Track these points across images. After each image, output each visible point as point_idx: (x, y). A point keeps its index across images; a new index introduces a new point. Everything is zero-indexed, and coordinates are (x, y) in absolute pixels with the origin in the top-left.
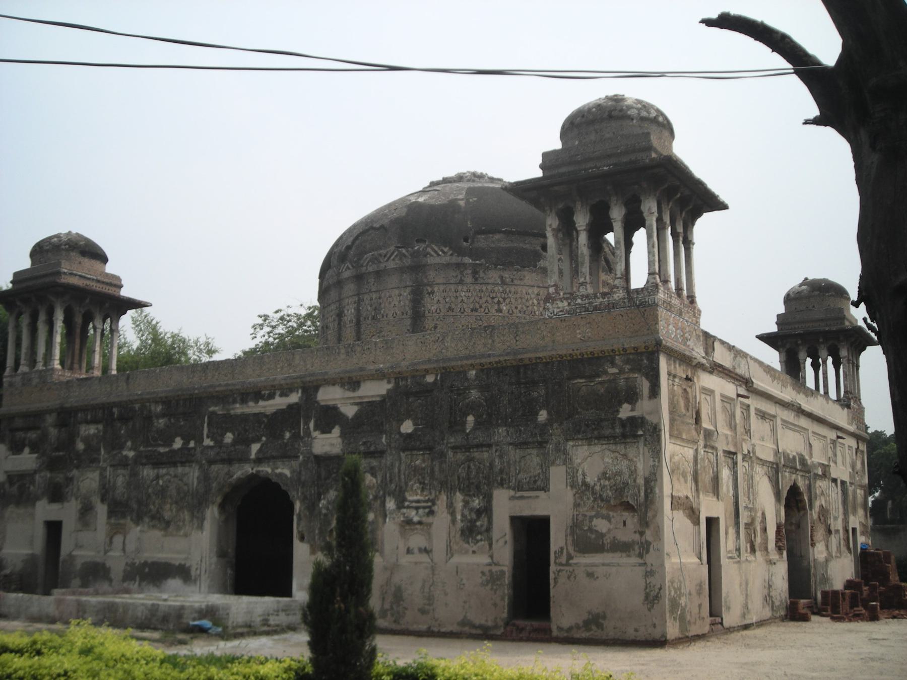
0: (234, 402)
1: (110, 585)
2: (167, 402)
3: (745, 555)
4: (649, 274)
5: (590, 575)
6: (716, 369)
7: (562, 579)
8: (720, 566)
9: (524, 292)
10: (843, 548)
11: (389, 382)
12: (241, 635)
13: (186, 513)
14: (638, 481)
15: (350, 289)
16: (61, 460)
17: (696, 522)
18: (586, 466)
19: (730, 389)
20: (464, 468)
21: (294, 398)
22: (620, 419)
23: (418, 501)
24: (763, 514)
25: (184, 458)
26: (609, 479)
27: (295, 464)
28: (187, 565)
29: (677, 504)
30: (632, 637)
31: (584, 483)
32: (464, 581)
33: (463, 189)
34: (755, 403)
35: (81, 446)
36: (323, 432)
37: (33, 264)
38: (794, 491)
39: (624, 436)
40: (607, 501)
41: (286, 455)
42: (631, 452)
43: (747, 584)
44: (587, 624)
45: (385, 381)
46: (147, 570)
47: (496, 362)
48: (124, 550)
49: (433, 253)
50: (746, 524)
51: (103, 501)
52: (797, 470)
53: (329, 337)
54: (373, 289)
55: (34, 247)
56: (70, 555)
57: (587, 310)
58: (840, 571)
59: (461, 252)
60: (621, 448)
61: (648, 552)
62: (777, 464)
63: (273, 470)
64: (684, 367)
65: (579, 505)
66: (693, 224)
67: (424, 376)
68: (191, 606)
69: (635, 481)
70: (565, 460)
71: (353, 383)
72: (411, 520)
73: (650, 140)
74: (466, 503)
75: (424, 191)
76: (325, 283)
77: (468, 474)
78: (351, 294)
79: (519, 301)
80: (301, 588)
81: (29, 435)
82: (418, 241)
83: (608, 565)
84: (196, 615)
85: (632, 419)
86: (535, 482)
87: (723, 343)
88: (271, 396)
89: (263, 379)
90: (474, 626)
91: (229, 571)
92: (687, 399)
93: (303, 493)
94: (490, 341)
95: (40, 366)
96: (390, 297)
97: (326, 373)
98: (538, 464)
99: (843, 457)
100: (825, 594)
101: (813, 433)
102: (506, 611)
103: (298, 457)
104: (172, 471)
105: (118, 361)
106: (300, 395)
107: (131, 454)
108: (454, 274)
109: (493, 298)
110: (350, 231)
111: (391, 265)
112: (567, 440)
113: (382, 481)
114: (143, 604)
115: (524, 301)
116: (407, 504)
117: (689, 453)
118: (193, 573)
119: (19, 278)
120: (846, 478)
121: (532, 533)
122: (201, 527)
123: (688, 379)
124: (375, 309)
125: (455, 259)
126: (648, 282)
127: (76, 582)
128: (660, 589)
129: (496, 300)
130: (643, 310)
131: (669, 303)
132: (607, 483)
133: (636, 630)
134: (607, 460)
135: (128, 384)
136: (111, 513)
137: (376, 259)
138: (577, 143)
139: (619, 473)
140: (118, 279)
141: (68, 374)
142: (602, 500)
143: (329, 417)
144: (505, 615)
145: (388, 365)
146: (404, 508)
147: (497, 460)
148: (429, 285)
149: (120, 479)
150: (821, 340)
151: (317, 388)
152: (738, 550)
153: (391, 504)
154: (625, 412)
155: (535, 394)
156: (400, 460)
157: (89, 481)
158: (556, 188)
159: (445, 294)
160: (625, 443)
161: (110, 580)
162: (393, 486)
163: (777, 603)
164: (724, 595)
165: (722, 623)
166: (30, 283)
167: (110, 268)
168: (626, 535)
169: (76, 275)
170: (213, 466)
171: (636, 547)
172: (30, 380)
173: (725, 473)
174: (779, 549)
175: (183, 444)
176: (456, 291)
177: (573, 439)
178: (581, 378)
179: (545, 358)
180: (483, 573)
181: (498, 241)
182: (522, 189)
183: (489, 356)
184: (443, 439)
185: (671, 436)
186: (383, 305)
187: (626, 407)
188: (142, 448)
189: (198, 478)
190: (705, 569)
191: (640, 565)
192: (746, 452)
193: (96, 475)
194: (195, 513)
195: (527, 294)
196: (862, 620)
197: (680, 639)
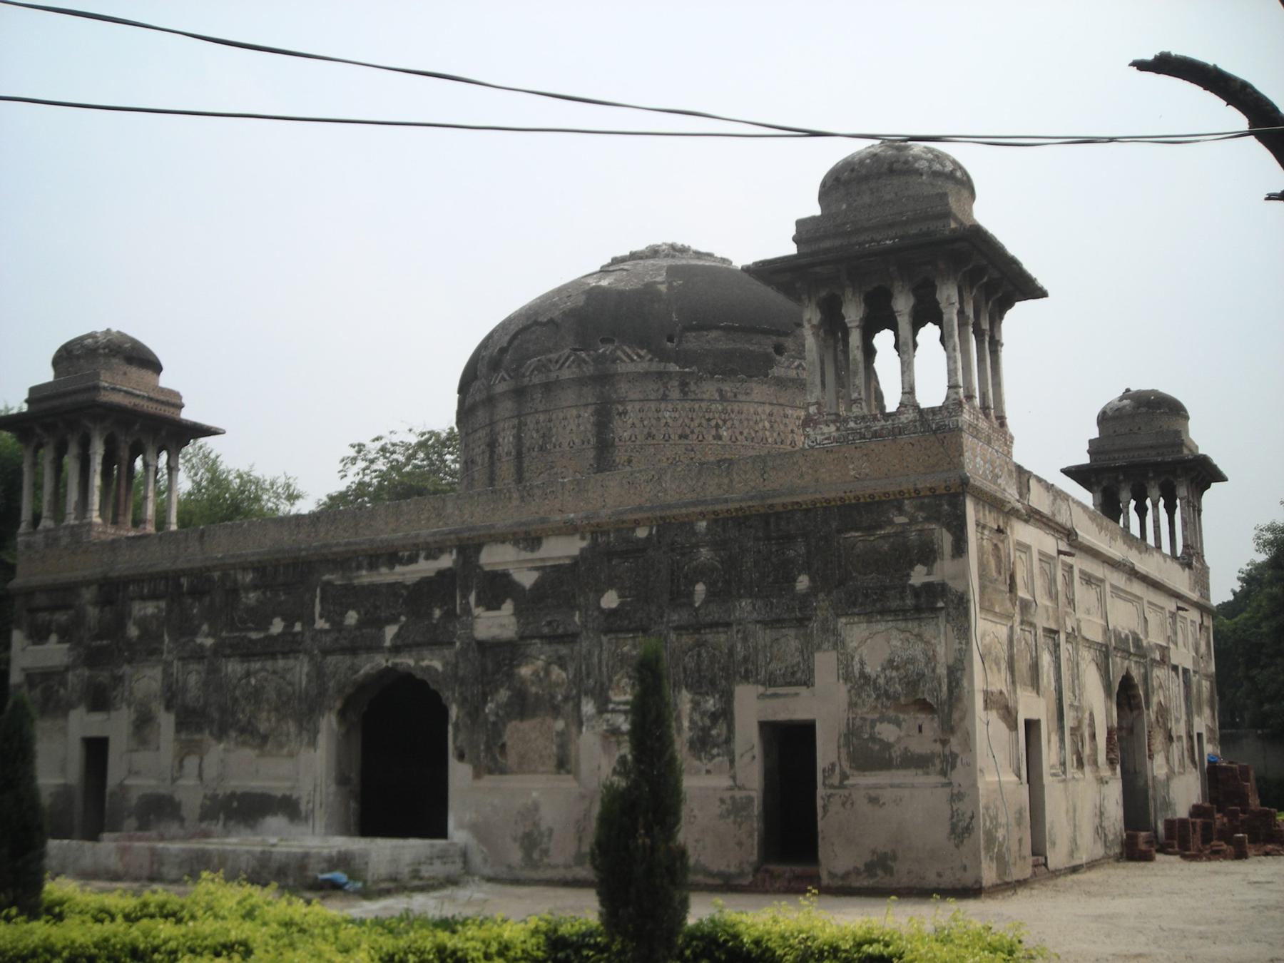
0: (359, 567)
1: (182, 826)
2: (260, 568)
3: (1072, 771)
4: (949, 387)
5: (874, 800)
6: (1034, 516)
7: (833, 809)
8: (1042, 787)
9: (752, 411)
10: (1187, 761)
11: (583, 538)
12: (386, 893)
13: (291, 723)
14: (938, 671)
15: (506, 408)
16: (106, 653)
17: (1013, 726)
18: (864, 651)
19: (1048, 543)
20: (692, 656)
21: (446, 561)
22: (912, 586)
24: (1091, 714)
25: (288, 646)
26: (897, 668)
27: (447, 652)
29: (991, 701)
30: (934, 885)
31: (863, 675)
32: (696, 812)
33: (661, 268)
34: (1080, 563)
35: (133, 632)
36: (489, 608)
37: (56, 376)
38: (1127, 682)
39: (918, 609)
40: (894, 698)
41: (436, 641)
42: (928, 631)
43: (1075, 811)
44: (870, 868)
45: (577, 537)
46: (235, 804)
47: (736, 510)
48: (200, 776)
49: (625, 358)
50: (1072, 729)
51: (168, 708)
52: (1130, 654)
53: (476, 476)
54: (541, 408)
55: (59, 351)
56: (122, 786)
57: (863, 437)
58: (1184, 792)
59: (664, 356)
61: (953, 767)
62: (1107, 647)
63: (417, 662)
64: (994, 514)
65: (856, 704)
66: (1001, 318)
67: (633, 530)
68: (319, 854)
69: (934, 670)
70: (835, 644)
71: (531, 540)
72: (619, 728)
73: (947, 204)
74: (696, 705)
75: (604, 271)
76: (469, 401)
77: (698, 665)
79: (745, 423)
80: (461, 826)
82: (603, 341)
83: (899, 786)
84: (324, 865)
85: (928, 587)
86: (793, 674)
87: (1039, 480)
88: (413, 559)
89: (400, 534)
90: (709, 874)
91: (353, 805)
92: (998, 559)
93: (461, 694)
94: (726, 481)
95: (71, 520)
96: (565, 418)
97: (493, 526)
98: (797, 649)
99: (1185, 637)
100: (1170, 824)
101: (1149, 603)
102: (755, 852)
103: (452, 644)
104: (269, 665)
105: (179, 513)
106: (454, 556)
107: (209, 642)
108: (655, 387)
109: (709, 420)
110: (503, 326)
111: (566, 374)
112: (838, 616)
113: (575, 676)
114: (248, 852)
115: (751, 423)
116: (611, 706)
117: (1003, 631)
118: (303, 807)
119: (36, 395)
120: (1189, 665)
121: (790, 746)
122: (313, 743)
123: (1000, 531)
125: (656, 366)
126: (947, 398)
127: (132, 823)
128: (972, 818)
129: (713, 423)
130: (941, 436)
131: (975, 427)
132: (894, 674)
133: (939, 875)
134: (894, 642)
136: (180, 726)
137: (544, 366)
138: (844, 206)
139: (912, 660)
140: (177, 395)
141: (111, 530)
142: (888, 698)
143: (497, 588)
144: (754, 857)
145: (581, 514)
146: (607, 711)
147: (739, 645)
148: (619, 402)
149: (193, 678)
150: (1151, 475)
151: (478, 548)
152: (1063, 764)
153: (588, 707)
154: (918, 576)
155: (792, 553)
156: (601, 645)
157: (147, 680)
158: (818, 269)
159: (640, 415)
160: (919, 619)
161: (182, 820)
162: (591, 682)
163: (1111, 837)
164: (1048, 826)
165: (1045, 865)
166: (56, 403)
167: (165, 381)
168: (924, 744)
169: (120, 391)
171: (937, 762)
172: (56, 539)
173: (1046, 659)
174: (1111, 762)
175: (285, 627)
176: (658, 411)
177: (847, 615)
178: (857, 531)
179: (805, 502)
180: (722, 801)
181: (715, 340)
182: (767, 271)
183: (726, 501)
184: (662, 617)
185: (981, 608)
186: (554, 430)
187: (920, 569)
188: (224, 634)
190: (1025, 790)
191: (944, 785)
192: (1070, 630)
193: (157, 672)
194: (305, 724)
195: (756, 413)
196: (1225, 858)
197: (998, 885)
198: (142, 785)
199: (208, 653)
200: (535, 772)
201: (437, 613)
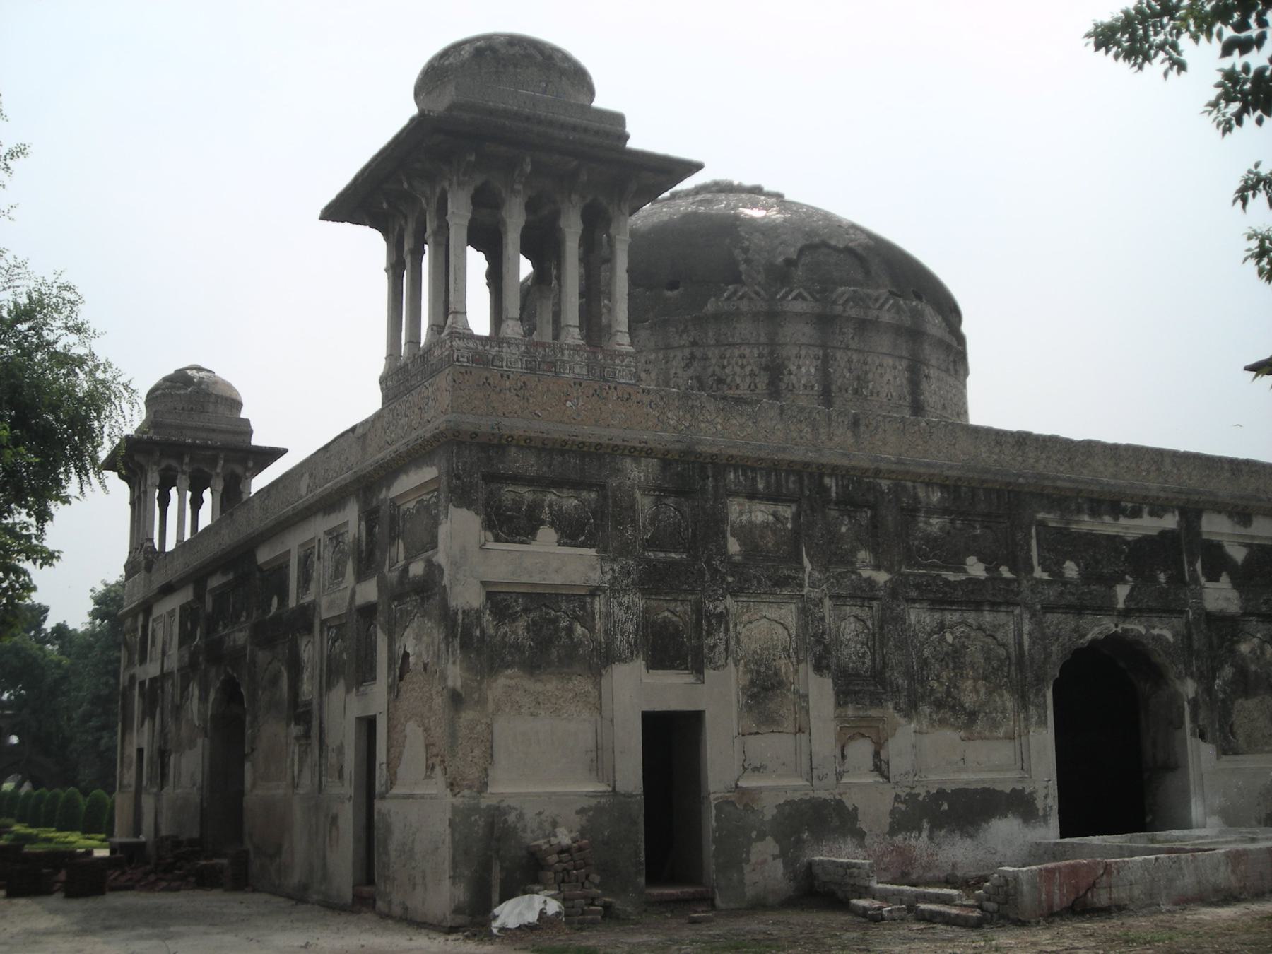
0: (1079, 511)
1: (861, 845)
2: (951, 487)
13: (1007, 696)
21: (1170, 522)
27: (1177, 622)
35: (734, 546)
36: (1209, 580)
41: (1168, 609)
51: (819, 668)
78: (804, 340)
81: (551, 497)
88: (1136, 513)
93: (1198, 668)
96: (881, 365)
103: (1182, 612)
104: (971, 617)
106: (1177, 518)
111: (887, 317)
124: (858, 378)
135: (856, 434)
136: (844, 695)
143: (1216, 561)
157: (765, 624)
170: (1048, 615)
186: (870, 376)
188: (904, 570)
189: (1030, 634)
193: (789, 613)
198: (778, 785)
200: (1262, 752)
201: (1162, 577)
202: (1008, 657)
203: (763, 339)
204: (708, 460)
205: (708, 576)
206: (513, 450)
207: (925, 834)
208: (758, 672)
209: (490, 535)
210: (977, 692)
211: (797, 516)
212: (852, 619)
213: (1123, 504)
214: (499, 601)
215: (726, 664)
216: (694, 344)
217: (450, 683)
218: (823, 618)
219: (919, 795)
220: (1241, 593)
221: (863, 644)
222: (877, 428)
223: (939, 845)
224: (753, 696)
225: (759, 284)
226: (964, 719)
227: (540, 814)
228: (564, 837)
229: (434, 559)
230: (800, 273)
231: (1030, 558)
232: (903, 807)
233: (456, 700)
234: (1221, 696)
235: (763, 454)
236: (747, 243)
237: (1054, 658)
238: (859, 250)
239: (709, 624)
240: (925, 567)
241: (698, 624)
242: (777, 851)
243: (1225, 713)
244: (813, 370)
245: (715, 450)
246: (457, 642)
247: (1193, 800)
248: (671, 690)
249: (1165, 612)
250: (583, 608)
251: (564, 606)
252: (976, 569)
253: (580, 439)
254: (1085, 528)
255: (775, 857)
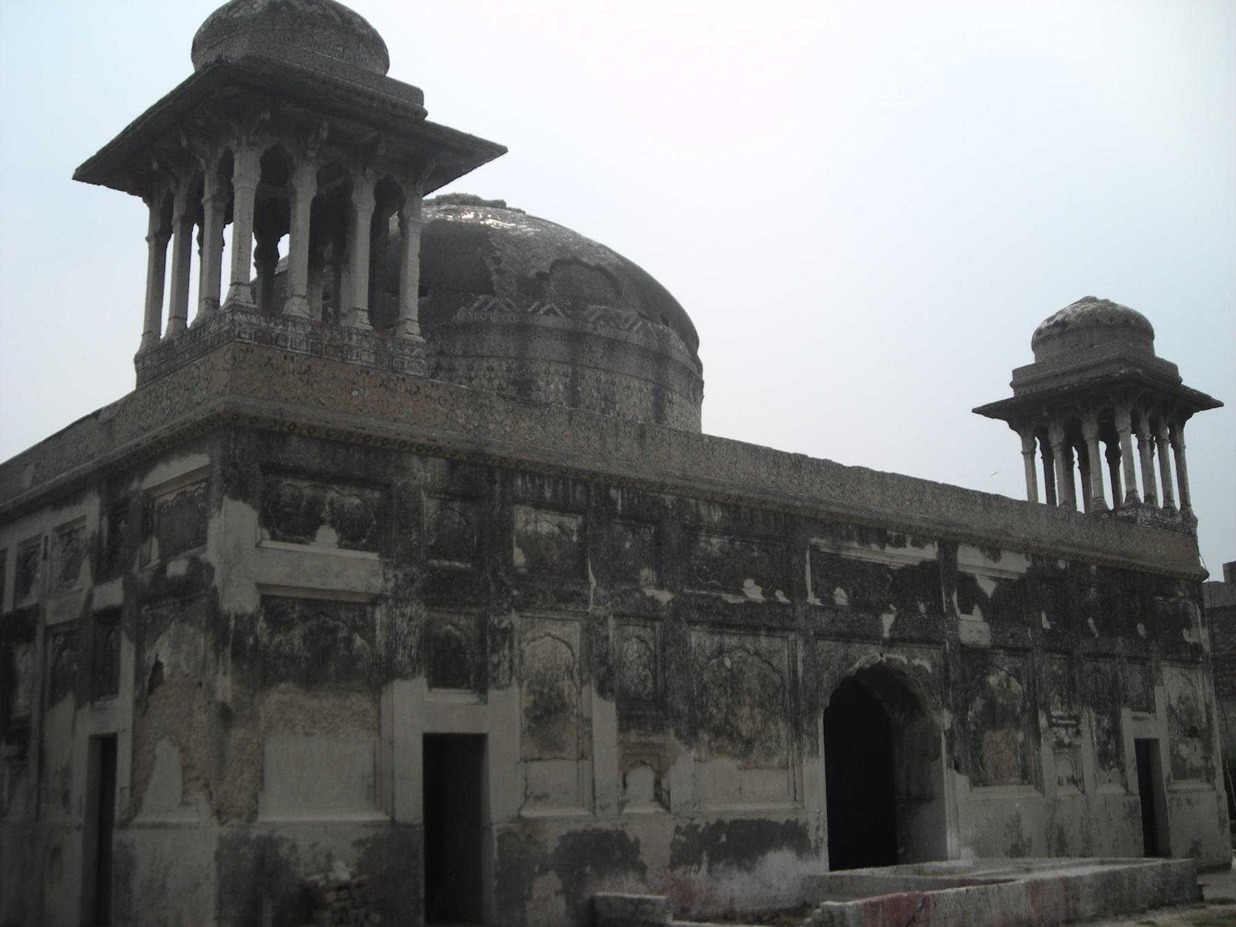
0: (850, 537)
1: (643, 880)
2: (731, 506)
13: (781, 724)
21: (930, 553)
23: (1062, 718)
27: (935, 653)
28: (801, 822)
36: (963, 612)
41: (928, 640)
46: (724, 839)
51: (603, 691)
60: (1186, 672)
81: (332, 494)
88: (900, 543)
93: (954, 699)
103: (940, 643)
104: (749, 642)
106: (936, 549)
111: (636, 338)
124: (606, 399)
136: (627, 720)
139: (1188, 698)
143: (970, 594)
153: (1043, 722)
157: (548, 643)
170: (820, 642)
186: (618, 397)
188: (686, 590)
189: (804, 661)
193: (573, 631)
198: (561, 817)
199: (664, 614)
201: (922, 607)
202: (783, 685)
203: (512, 353)
204: (497, 463)
205: (493, 588)
206: (295, 439)
207: (704, 867)
208: (541, 694)
209: (266, 532)
210: (754, 720)
211: (583, 529)
212: (634, 640)
213: (889, 533)
214: (275, 606)
215: (510, 684)
216: (441, 353)
217: (219, 697)
218: (607, 638)
219: (699, 826)
220: (991, 625)
221: (645, 667)
222: (662, 440)
223: (717, 879)
224: (536, 720)
225: (511, 296)
226: (741, 747)
227: (314, 845)
228: (342, 873)
229: (202, 557)
230: (551, 288)
231: (804, 583)
232: (683, 839)
233: (226, 716)
234: (973, 728)
235: (552, 461)
236: (499, 254)
237: (825, 685)
238: (610, 269)
239: (494, 640)
240: (706, 588)
241: (482, 639)
242: (558, 884)
243: (976, 745)
244: (561, 387)
245: (504, 453)
246: (228, 651)
247: (948, 832)
248: (454, 711)
249: (923, 642)
250: (363, 617)
251: (343, 614)
252: (753, 592)
253: (366, 432)
254: (854, 555)
255: (557, 893)
